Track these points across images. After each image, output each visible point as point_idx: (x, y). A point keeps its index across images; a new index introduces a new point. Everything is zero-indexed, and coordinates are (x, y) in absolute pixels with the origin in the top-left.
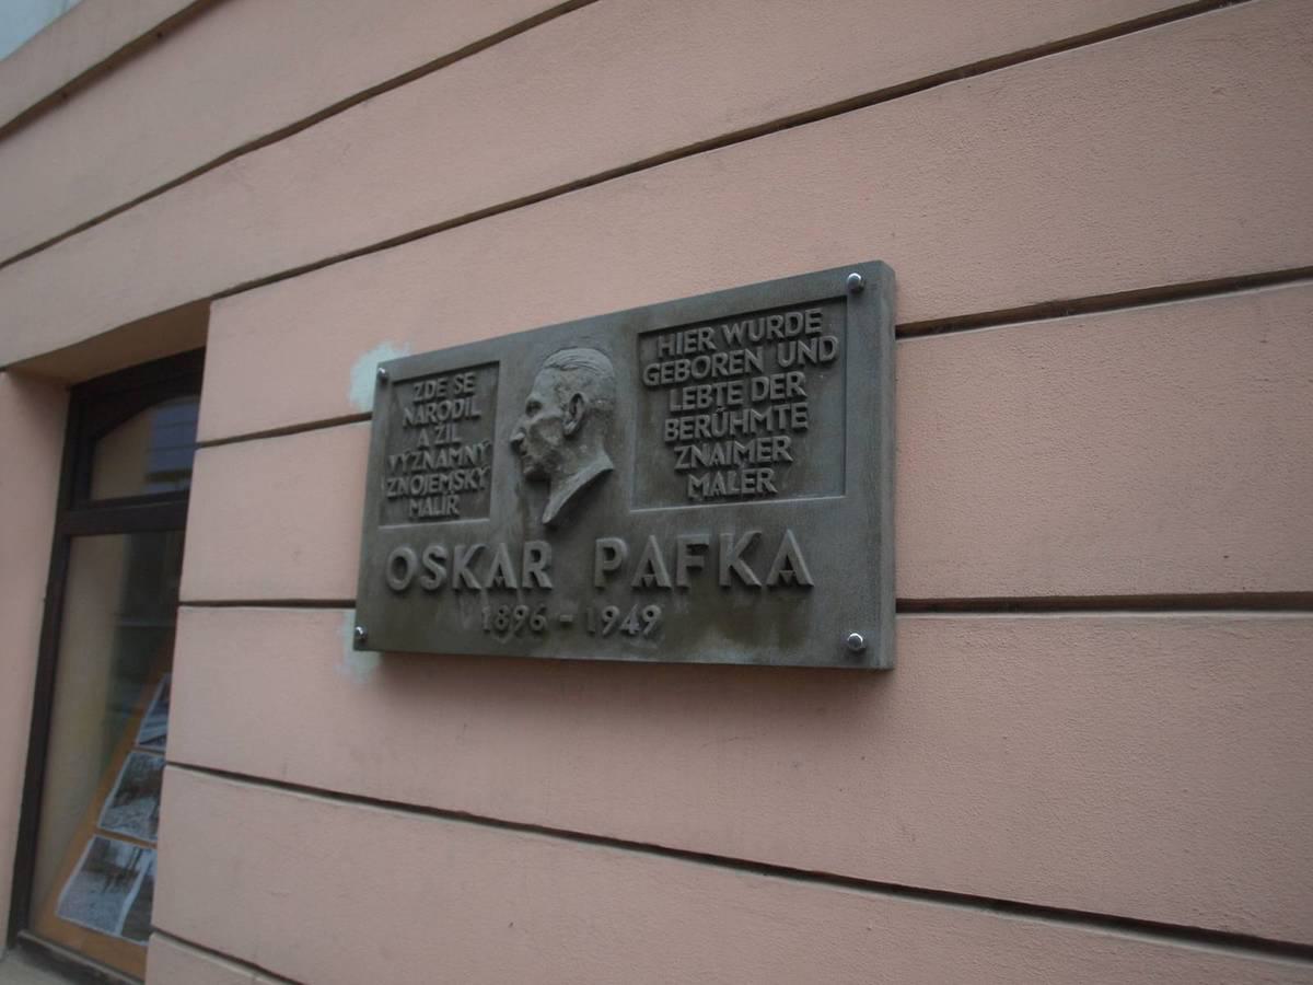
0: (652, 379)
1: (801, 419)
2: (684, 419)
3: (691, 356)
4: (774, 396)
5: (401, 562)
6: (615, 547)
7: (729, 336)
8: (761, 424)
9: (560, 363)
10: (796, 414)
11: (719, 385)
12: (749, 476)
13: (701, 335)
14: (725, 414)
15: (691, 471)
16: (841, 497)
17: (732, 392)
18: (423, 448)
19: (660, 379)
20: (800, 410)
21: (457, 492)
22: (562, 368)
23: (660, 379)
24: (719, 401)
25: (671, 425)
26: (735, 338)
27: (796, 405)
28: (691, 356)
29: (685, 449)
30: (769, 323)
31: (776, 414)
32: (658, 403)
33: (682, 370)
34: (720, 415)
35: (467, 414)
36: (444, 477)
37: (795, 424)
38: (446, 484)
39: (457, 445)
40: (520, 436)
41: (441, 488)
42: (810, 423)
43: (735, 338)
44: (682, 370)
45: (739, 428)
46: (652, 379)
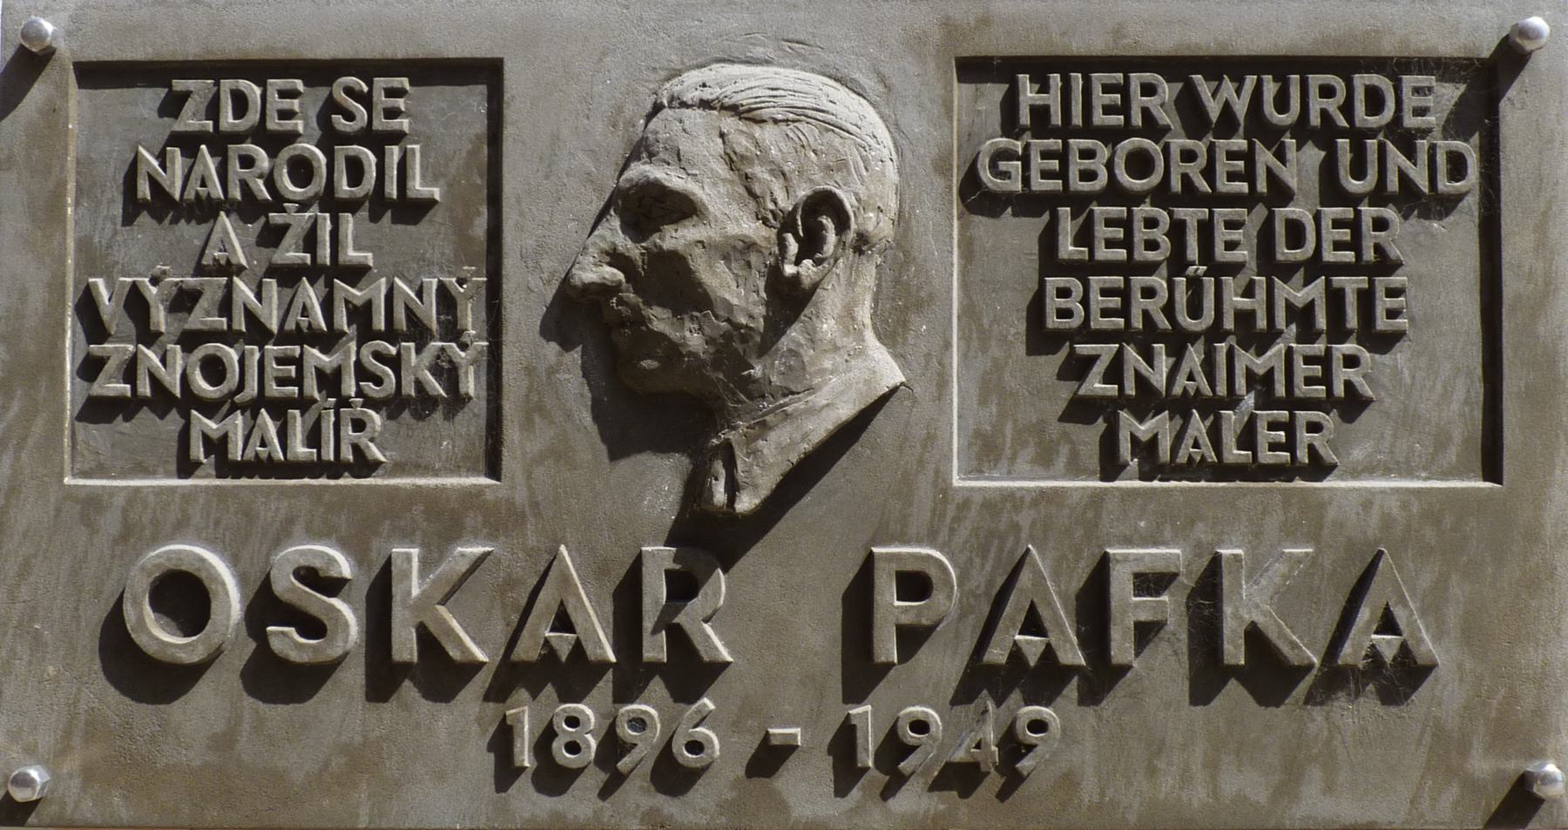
0: (1005, 175)
1: (1392, 314)
2: (1096, 282)
3: (1111, 136)
4: (1329, 256)
5: (184, 596)
6: (933, 572)
7: (1214, 109)
8: (1302, 315)
9: (743, 99)
10: (1383, 303)
11: (1191, 216)
12: (1273, 426)
13: (1135, 88)
14: (1209, 282)
15: (1121, 401)
16: (1488, 485)
17: (1222, 235)
18: (228, 269)
19: (1026, 181)
20: (1393, 293)
21: (370, 403)
22: (747, 114)
23: (1026, 181)
24: (1193, 252)
25: (1064, 293)
26: (1227, 109)
27: (1381, 282)
28: (1111, 136)
29: (1107, 351)
30: (1314, 91)
31: (1335, 298)
32: (1017, 236)
33: (1087, 164)
34: (1195, 285)
35: (392, 190)
36: (316, 356)
37: (1382, 323)
38: (330, 381)
39: (356, 274)
40: (612, 274)
41: (311, 388)
42: (1412, 319)
43: (1227, 109)
44: (1087, 164)
45: (1245, 317)
46: (1005, 175)
